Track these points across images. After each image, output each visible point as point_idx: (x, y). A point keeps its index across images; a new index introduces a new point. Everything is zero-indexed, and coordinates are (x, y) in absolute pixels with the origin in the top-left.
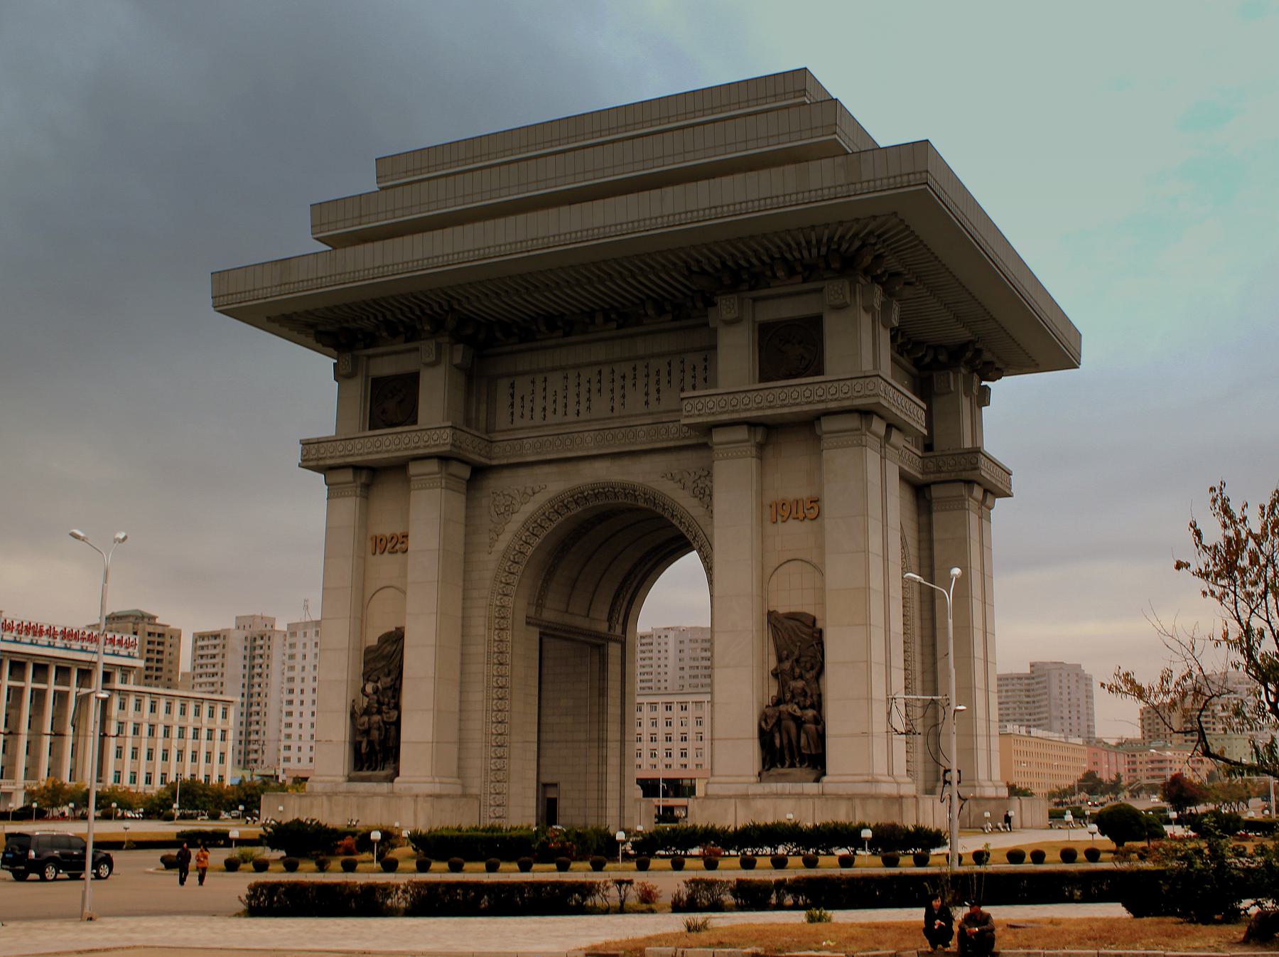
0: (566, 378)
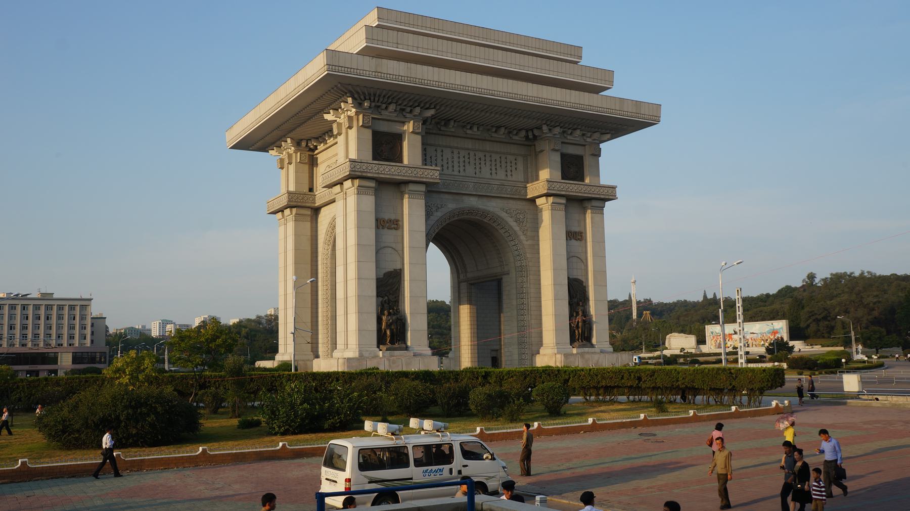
0: (453, 152)
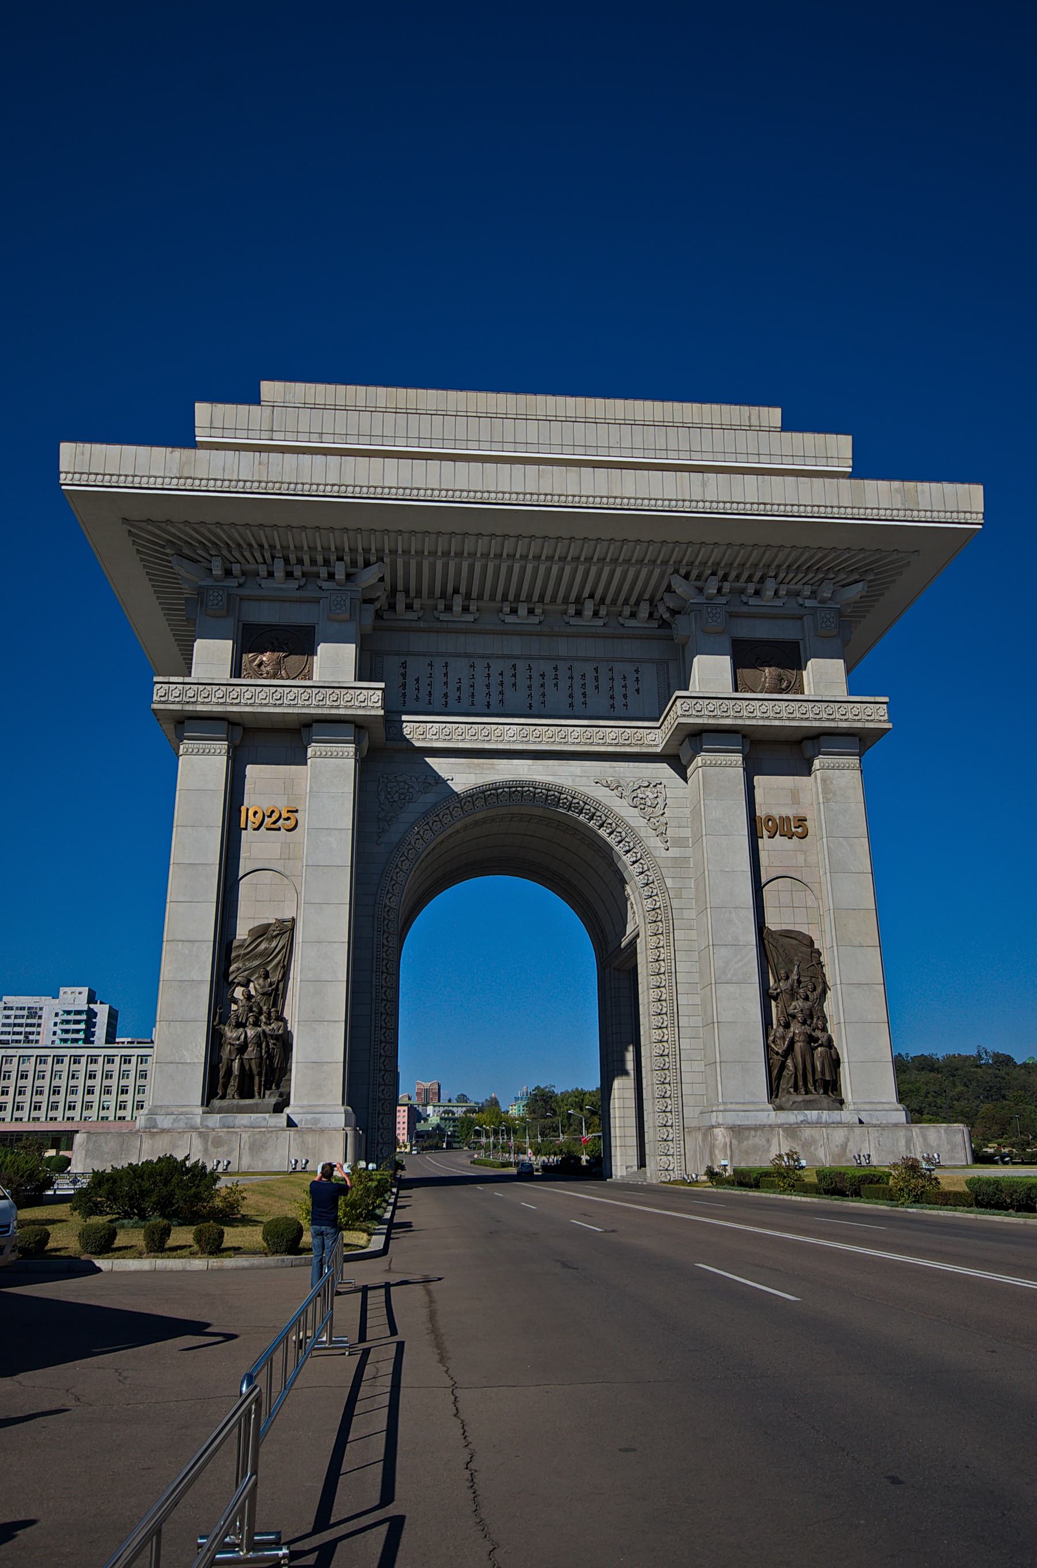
0: (473, 666)
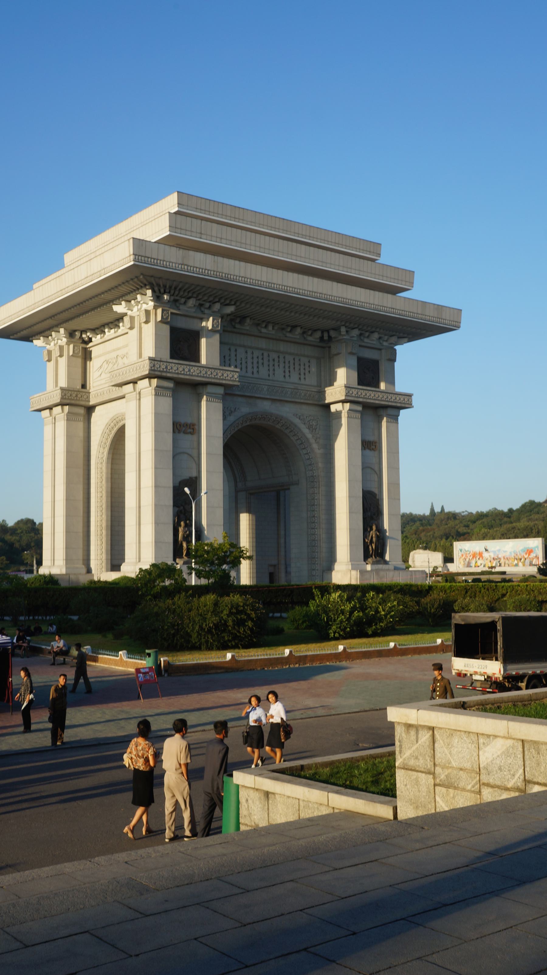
0: (246, 352)
